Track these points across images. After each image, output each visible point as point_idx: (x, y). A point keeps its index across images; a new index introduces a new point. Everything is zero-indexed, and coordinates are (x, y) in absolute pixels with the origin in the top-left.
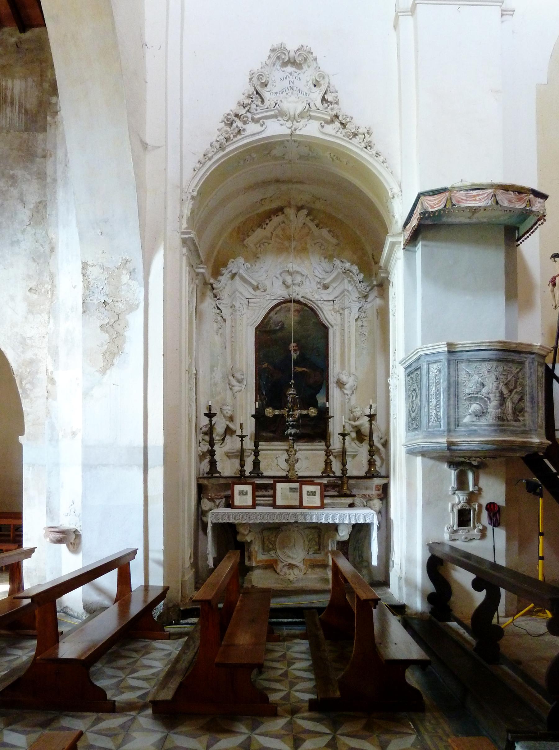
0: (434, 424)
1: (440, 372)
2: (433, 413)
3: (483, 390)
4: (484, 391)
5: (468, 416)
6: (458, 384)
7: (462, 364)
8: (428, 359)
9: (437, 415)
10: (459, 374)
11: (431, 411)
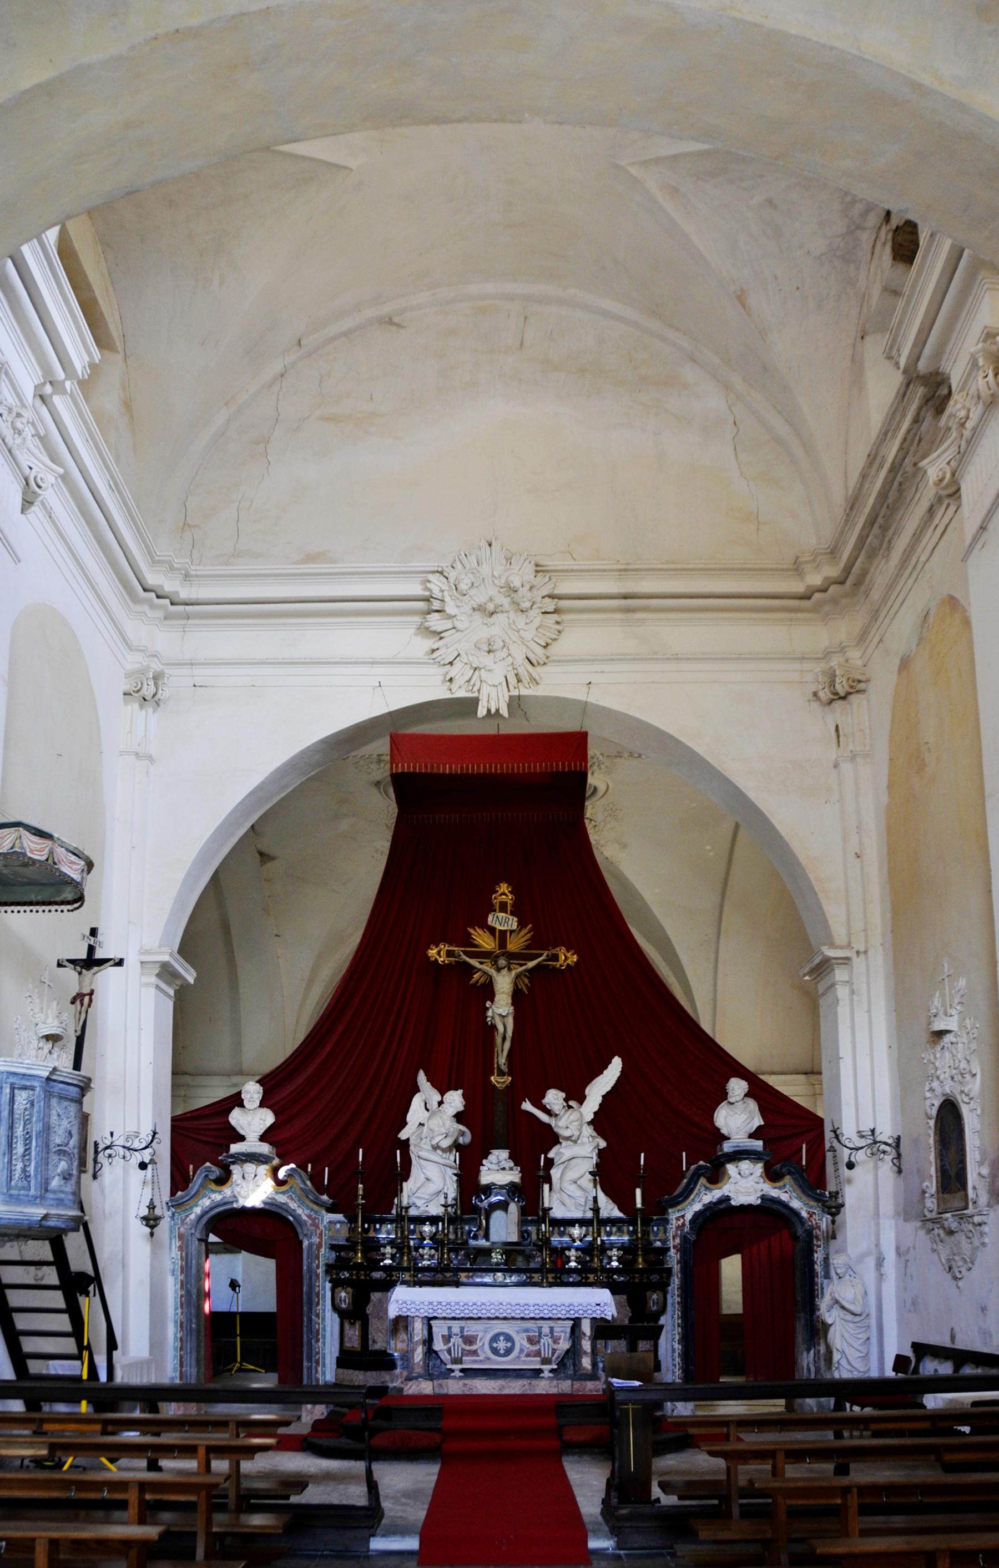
0: (20, 1184)
1: (32, 1105)
2: (19, 1166)
5: (57, 1178)
8: (11, 1080)
9: (24, 1170)
11: (14, 1162)
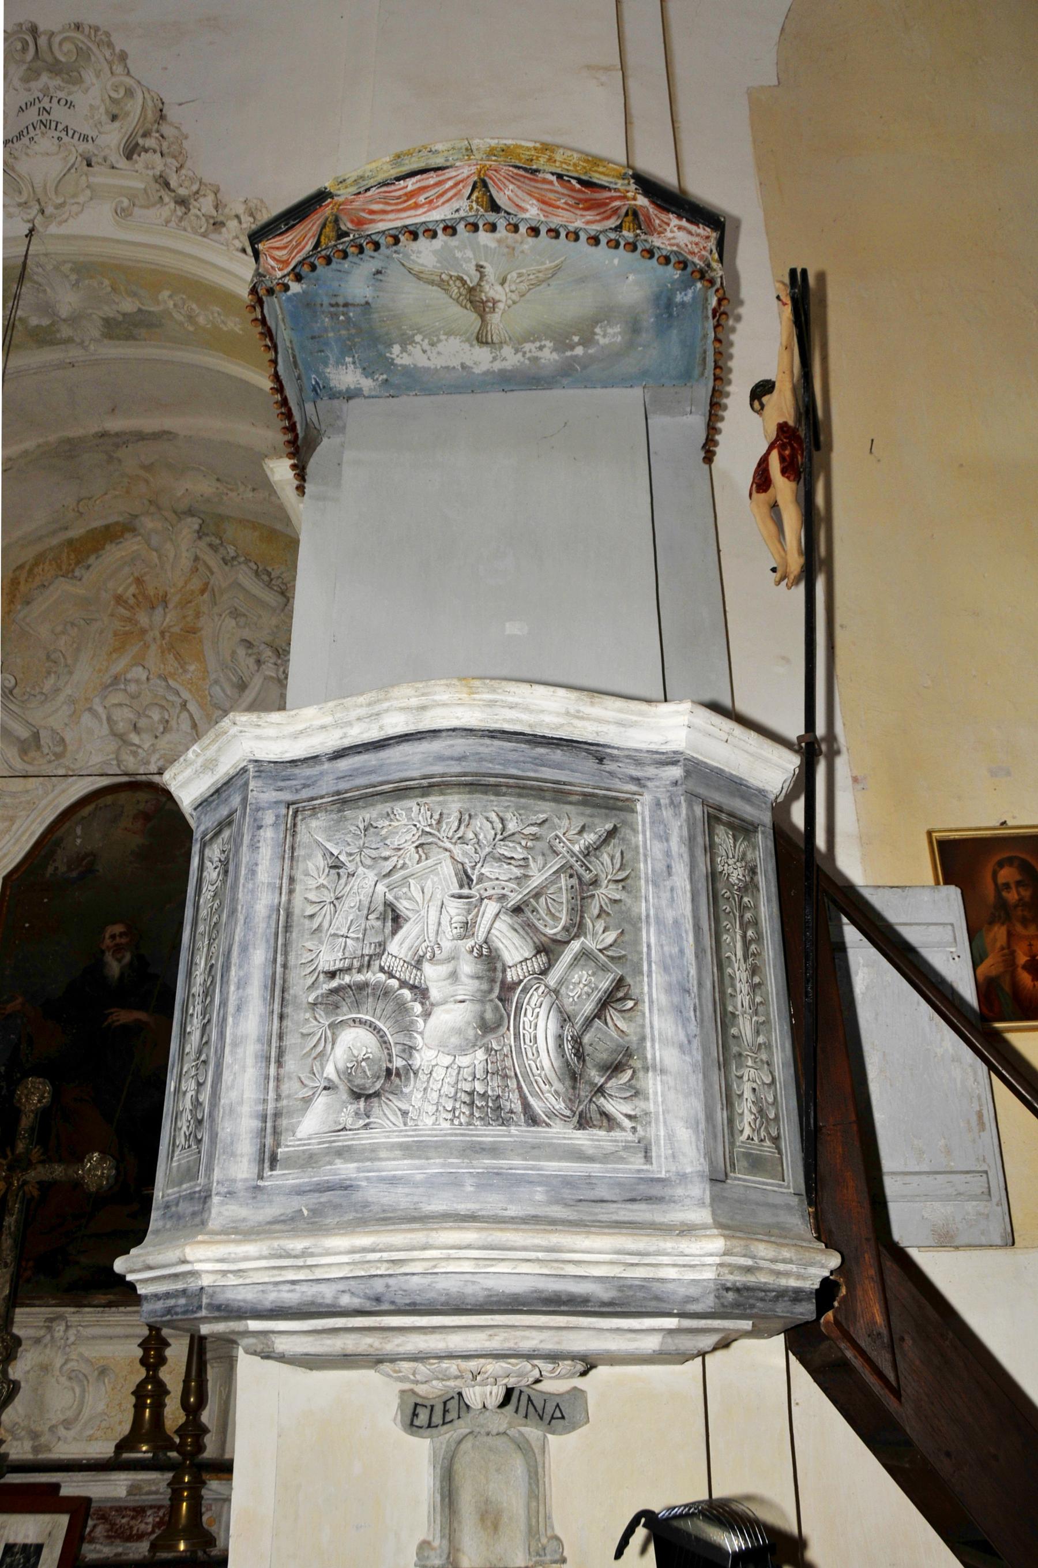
3: (393, 947)
4: (399, 947)
5: (322, 1101)
6: (287, 928)
7: (314, 823)
10: (299, 876)
